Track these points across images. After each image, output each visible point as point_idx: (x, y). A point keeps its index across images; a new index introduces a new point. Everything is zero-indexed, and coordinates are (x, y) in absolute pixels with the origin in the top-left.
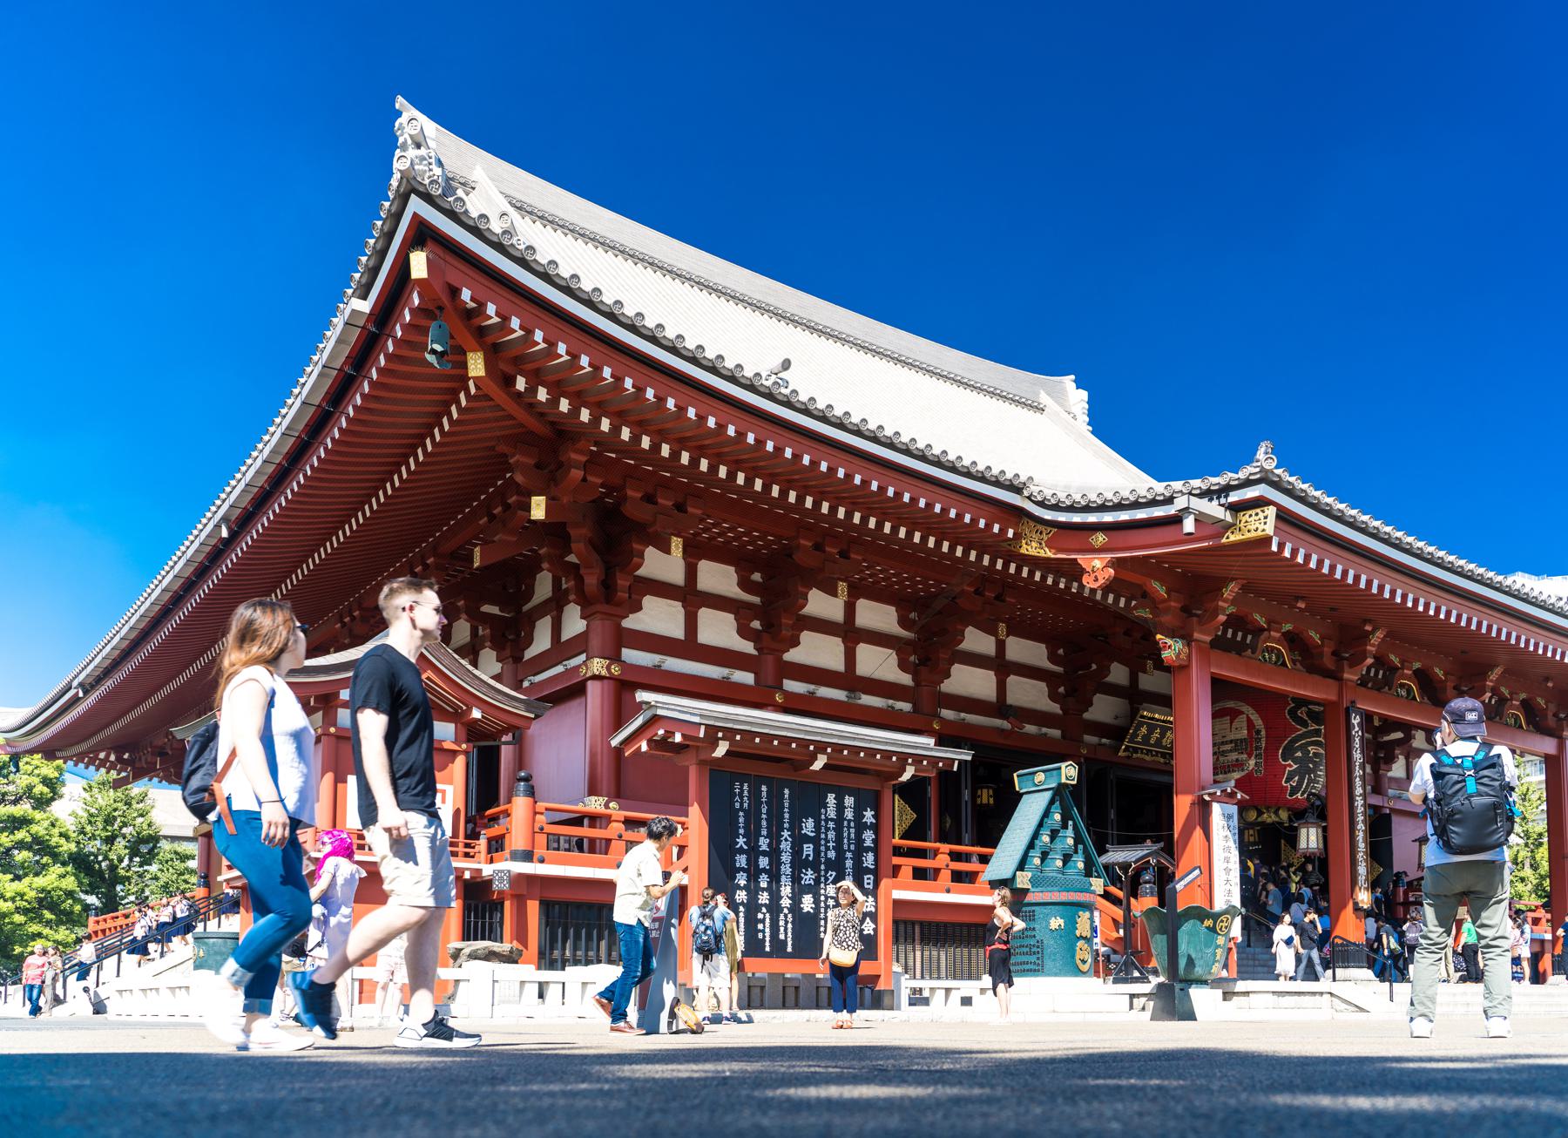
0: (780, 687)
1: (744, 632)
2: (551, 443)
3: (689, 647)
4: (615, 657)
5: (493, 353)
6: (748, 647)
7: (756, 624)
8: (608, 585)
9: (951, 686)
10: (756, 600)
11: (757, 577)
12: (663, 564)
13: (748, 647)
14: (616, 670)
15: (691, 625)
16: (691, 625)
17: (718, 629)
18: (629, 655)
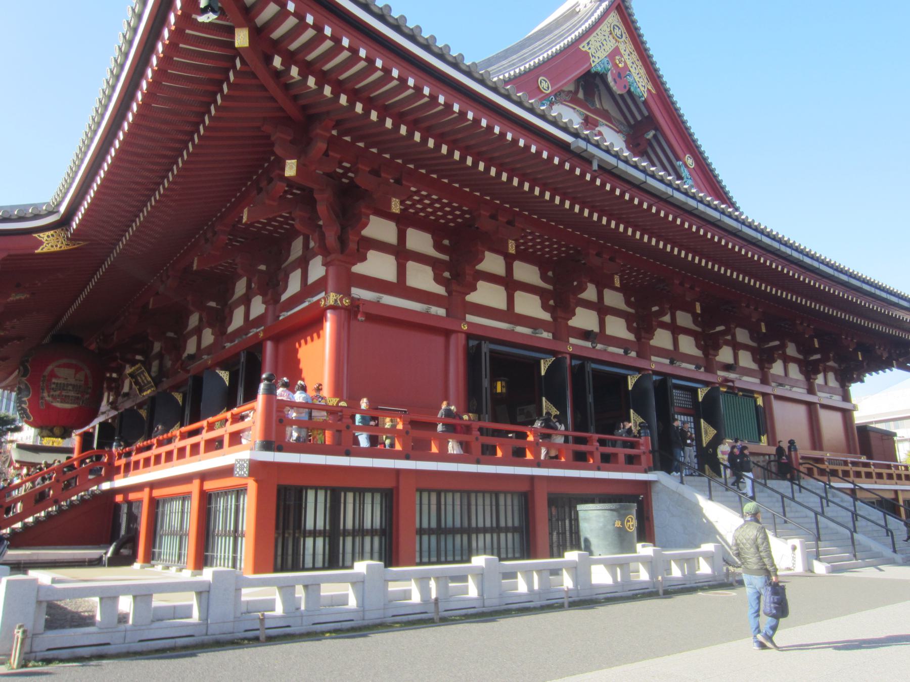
0: (464, 319)
1: (438, 279)
2: (302, 121)
3: (400, 288)
4: (348, 294)
5: (258, 33)
6: (440, 290)
7: (447, 274)
8: (342, 241)
9: (574, 322)
10: (446, 258)
11: (446, 242)
12: (380, 229)
13: (440, 290)
14: (346, 302)
15: (401, 272)
16: (401, 272)
17: (421, 277)
18: (357, 292)
